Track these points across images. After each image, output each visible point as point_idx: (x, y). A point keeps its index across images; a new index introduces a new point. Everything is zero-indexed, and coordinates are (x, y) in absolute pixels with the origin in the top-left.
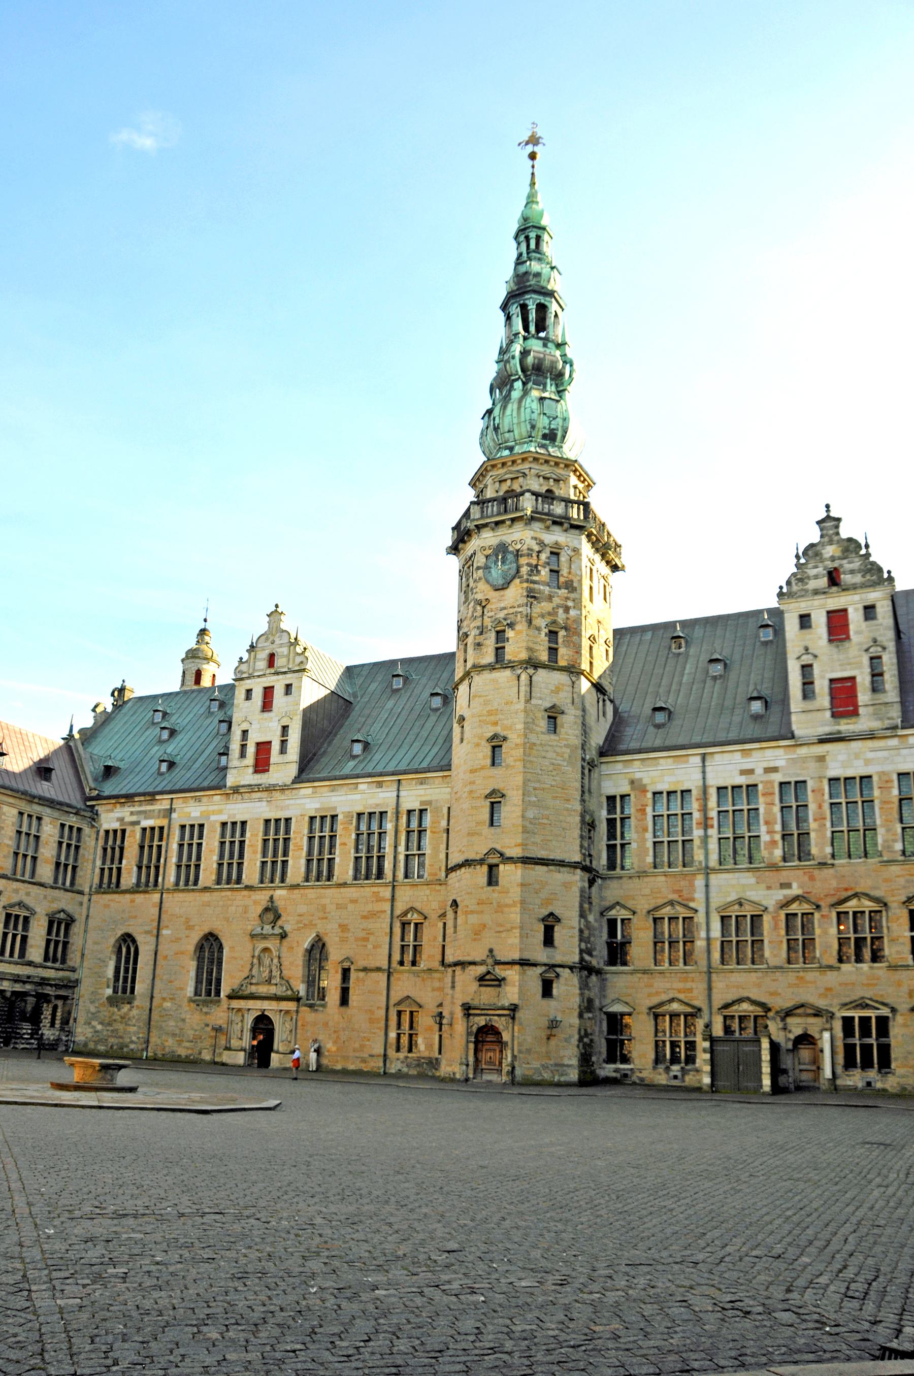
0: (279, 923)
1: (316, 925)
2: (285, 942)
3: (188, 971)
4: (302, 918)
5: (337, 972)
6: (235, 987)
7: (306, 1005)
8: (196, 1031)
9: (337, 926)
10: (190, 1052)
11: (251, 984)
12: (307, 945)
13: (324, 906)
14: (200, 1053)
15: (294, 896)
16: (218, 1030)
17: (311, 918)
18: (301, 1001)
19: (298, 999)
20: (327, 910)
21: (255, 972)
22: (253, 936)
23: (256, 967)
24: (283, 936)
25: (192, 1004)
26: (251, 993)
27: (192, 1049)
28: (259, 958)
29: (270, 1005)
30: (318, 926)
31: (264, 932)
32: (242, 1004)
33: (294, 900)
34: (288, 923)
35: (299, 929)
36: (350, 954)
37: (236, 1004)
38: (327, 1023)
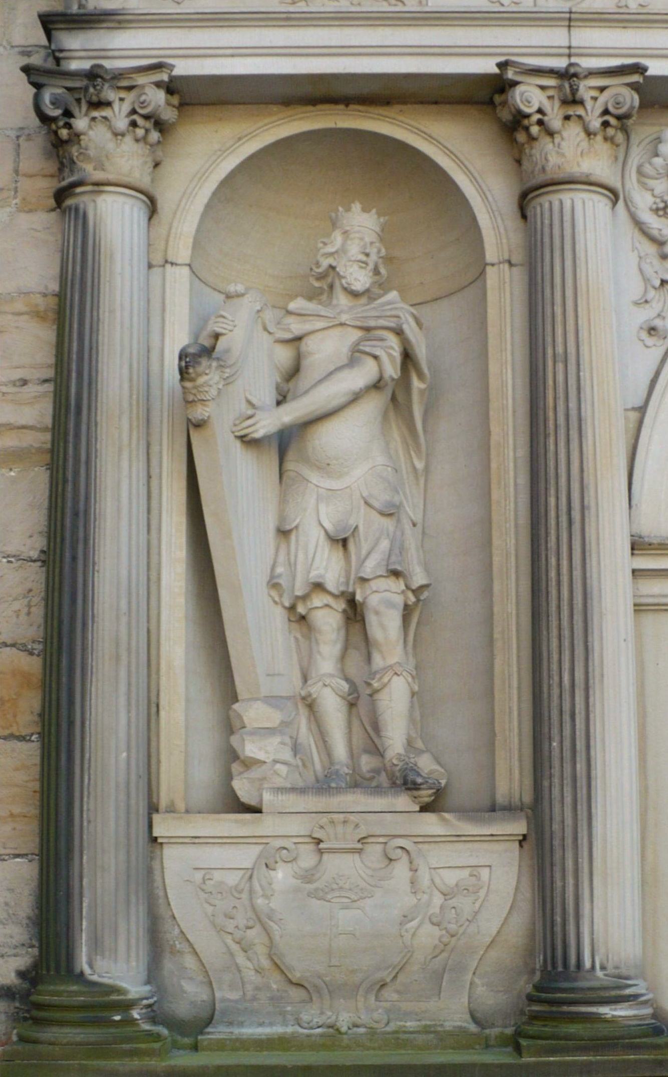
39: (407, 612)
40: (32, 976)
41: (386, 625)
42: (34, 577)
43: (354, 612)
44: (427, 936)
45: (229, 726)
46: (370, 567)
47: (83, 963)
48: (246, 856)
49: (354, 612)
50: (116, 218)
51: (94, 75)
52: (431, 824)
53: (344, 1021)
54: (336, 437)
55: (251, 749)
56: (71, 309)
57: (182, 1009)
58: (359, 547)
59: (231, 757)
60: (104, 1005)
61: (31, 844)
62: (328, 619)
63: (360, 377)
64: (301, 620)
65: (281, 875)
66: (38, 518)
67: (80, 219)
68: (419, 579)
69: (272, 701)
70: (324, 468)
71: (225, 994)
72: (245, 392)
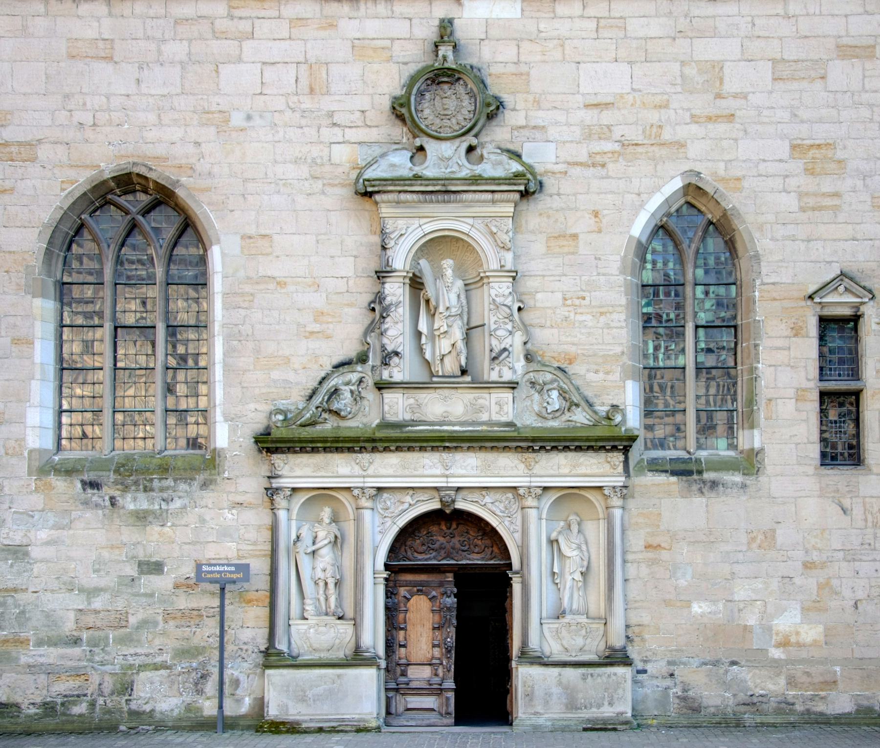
0: (498, 134)
1: (681, 145)
2: (535, 214)
3: (24, 342)
4: (607, 117)
5: (797, 331)
6: (294, 400)
7: (655, 466)
8: (92, 592)
9: (784, 150)
10: (63, 686)
11: (381, 386)
12: (639, 226)
13: (715, 70)
14: (126, 688)
15: (563, 28)
16: (224, 584)
17: (654, 117)
18: (637, 449)
19: (622, 444)
20: (731, 86)
21: (397, 332)
22: (367, 193)
23: (400, 315)
24: (527, 188)
25: (59, 483)
26: (385, 425)
27: (77, 673)
28: (416, 283)
29: (486, 470)
30: (695, 150)
31: (430, 170)
32: (341, 470)
33: (562, 42)
34: (543, 130)
35: (595, 162)
36: (858, 258)
37: (301, 471)
38: (770, 535)
39: (336, 584)
40: (267, 649)
41: (331, 586)
42: (268, 578)
43: (326, 584)
44: (337, 641)
45: (303, 604)
46: (329, 575)
47: (277, 646)
48: (305, 627)
49: (326, 584)
50: (282, 515)
51: (277, 489)
52: (339, 622)
53: (322, 656)
54: (323, 551)
55: (307, 608)
56: (274, 529)
57: (294, 654)
58: (327, 572)
59: (303, 610)
60: (280, 653)
61: (268, 625)
62: (322, 584)
63: (326, 542)
64: (316, 583)
65: (312, 630)
66: (269, 567)
67: (275, 514)
68: (338, 577)
69: (311, 599)
70: (321, 557)
71: (302, 651)
72: (306, 544)
